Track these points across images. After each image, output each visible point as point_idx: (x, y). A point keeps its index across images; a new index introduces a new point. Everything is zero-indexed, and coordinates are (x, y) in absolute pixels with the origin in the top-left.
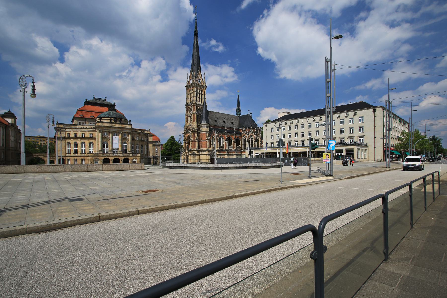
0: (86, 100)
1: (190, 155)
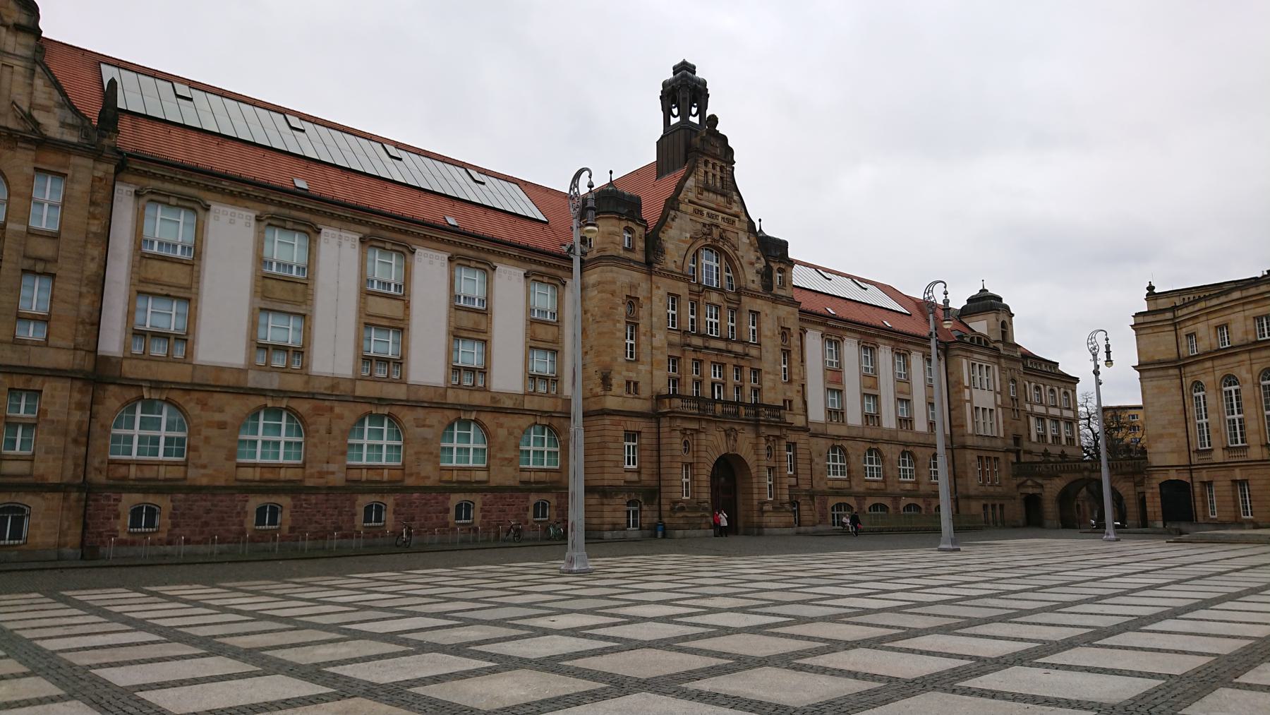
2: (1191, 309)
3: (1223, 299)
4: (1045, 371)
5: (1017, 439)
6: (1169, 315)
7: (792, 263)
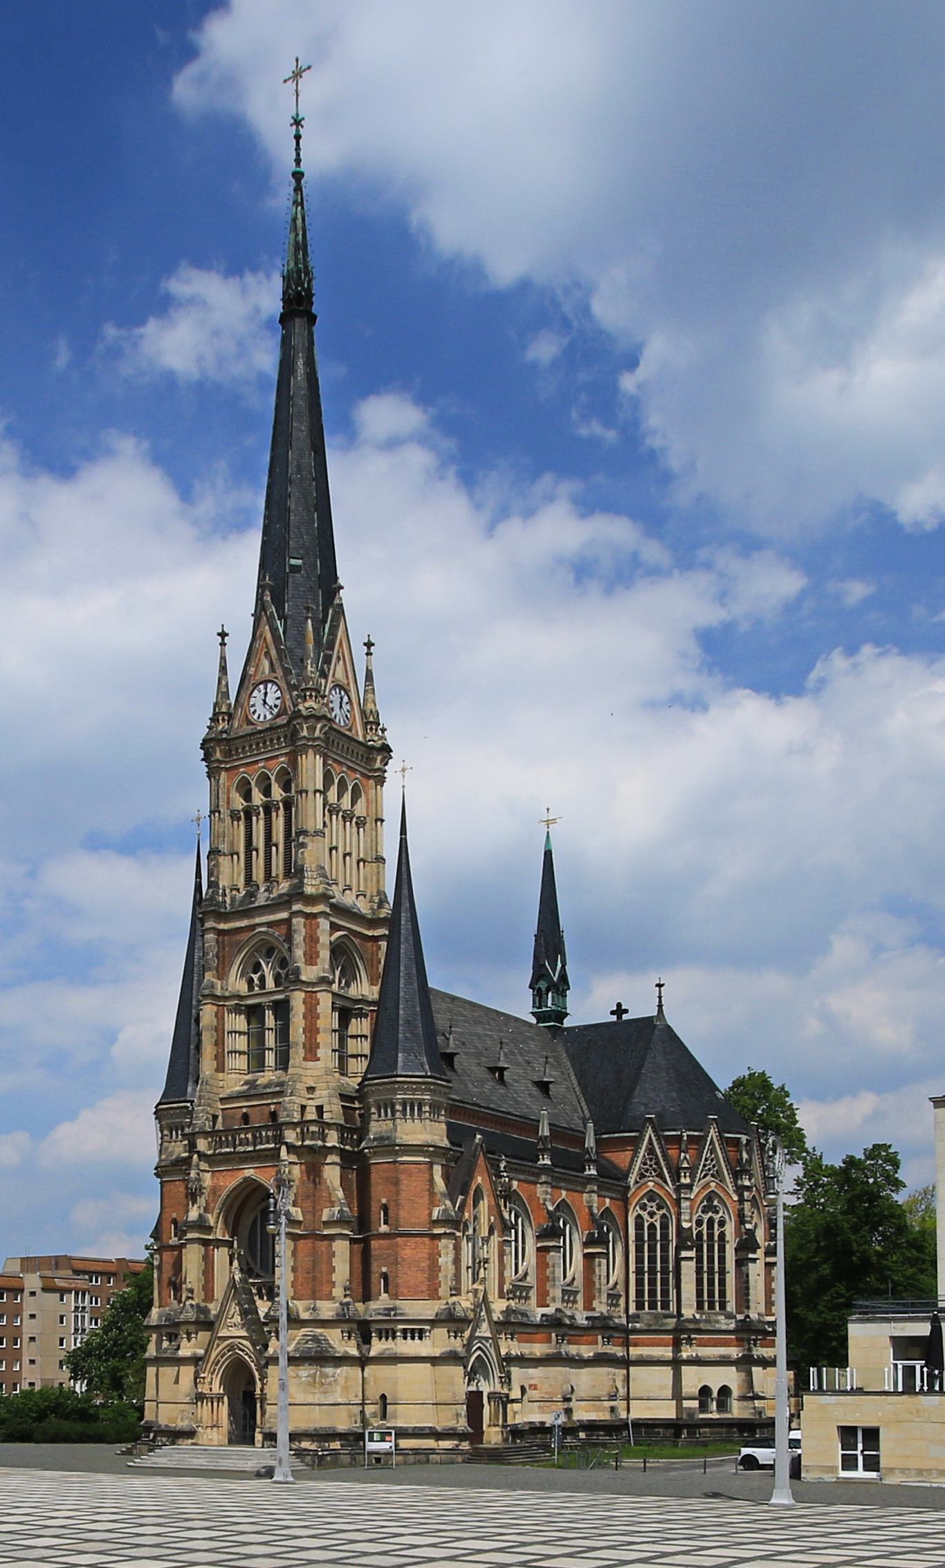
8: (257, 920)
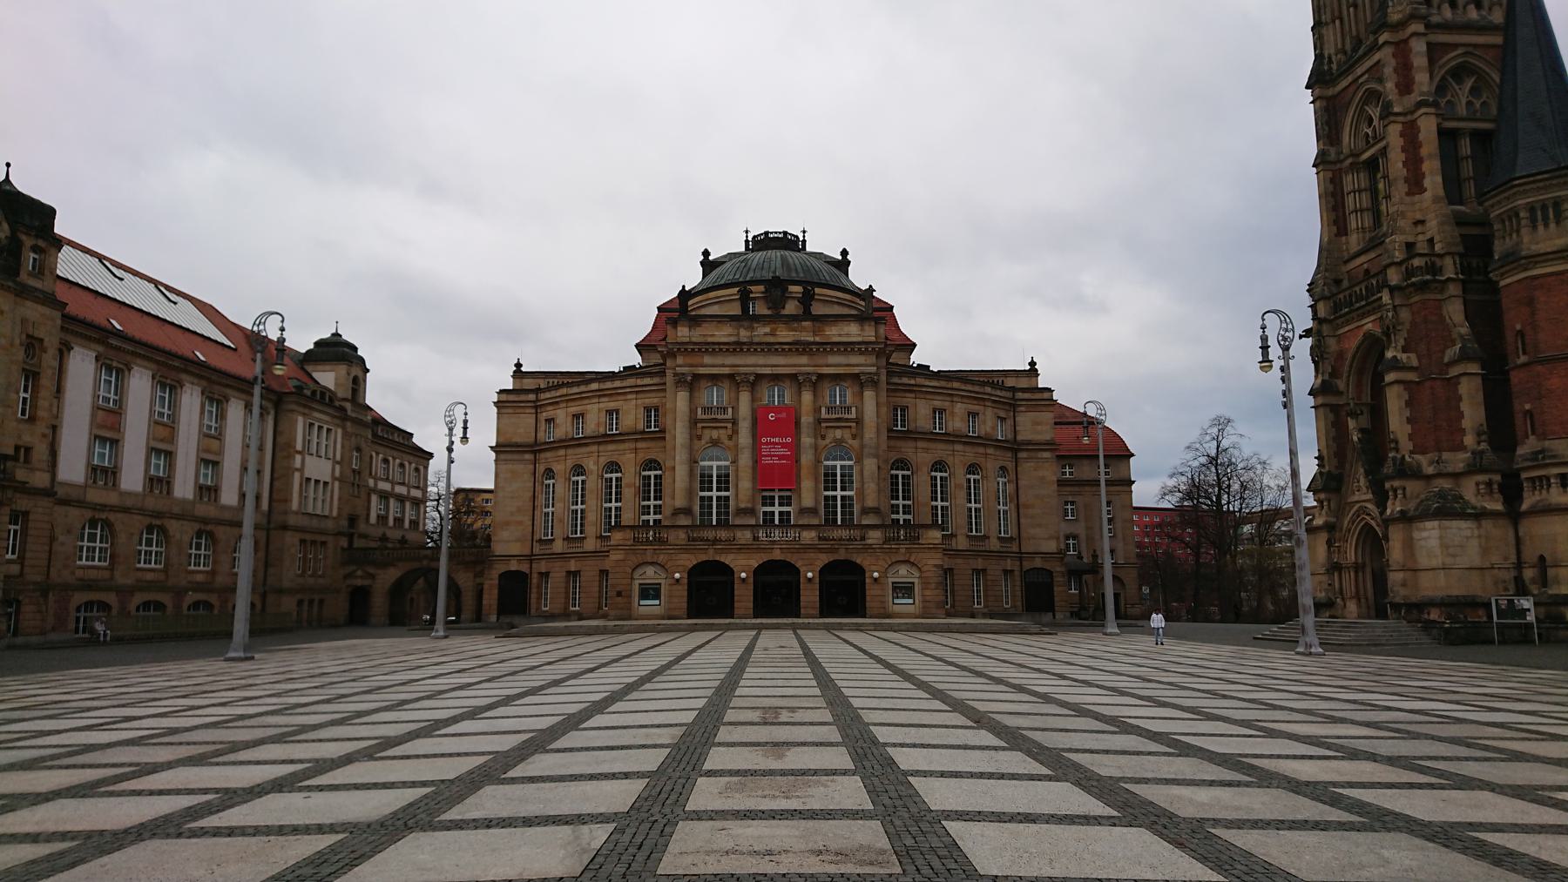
0: (706, 253)
1: (1405, 518)
2: (553, 394)
3: (583, 388)
4: (399, 443)
5: (353, 520)
6: (532, 397)
7: (59, 242)
8: (1359, 71)
